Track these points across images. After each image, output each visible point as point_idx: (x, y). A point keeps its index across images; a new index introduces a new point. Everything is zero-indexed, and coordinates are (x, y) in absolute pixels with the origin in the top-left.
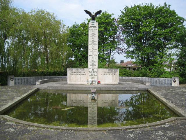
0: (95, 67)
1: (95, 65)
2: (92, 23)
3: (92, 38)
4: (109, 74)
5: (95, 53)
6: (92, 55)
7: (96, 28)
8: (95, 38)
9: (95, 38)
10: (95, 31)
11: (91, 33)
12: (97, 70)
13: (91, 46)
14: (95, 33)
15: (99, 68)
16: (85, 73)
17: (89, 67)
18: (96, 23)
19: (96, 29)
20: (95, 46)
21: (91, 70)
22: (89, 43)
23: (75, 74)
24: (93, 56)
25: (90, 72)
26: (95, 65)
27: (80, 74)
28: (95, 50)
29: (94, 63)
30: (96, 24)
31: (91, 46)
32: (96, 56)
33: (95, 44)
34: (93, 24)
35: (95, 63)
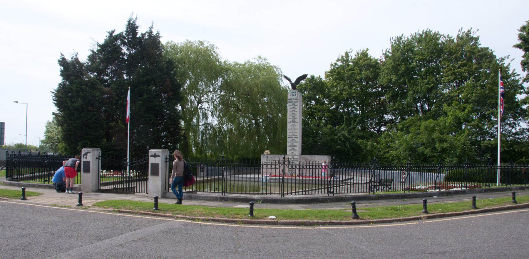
0: (295, 153)
1: (295, 150)
2: (292, 94)
3: (291, 113)
5: (295, 134)
6: (291, 137)
7: (297, 99)
8: (296, 113)
9: (296, 113)
10: (296, 104)
11: (291, 107)
12: (298, 157)
13: (291, 124)
14: (296, 107)
18: (296, 94)
19: (297, 101)
20: (296, 124)
22: (289, 120)
24: (294, 138)
26: (295, 150)
29: (294, 147)
31: (291, 124)
34: (293, 94)
35: (295, 148)
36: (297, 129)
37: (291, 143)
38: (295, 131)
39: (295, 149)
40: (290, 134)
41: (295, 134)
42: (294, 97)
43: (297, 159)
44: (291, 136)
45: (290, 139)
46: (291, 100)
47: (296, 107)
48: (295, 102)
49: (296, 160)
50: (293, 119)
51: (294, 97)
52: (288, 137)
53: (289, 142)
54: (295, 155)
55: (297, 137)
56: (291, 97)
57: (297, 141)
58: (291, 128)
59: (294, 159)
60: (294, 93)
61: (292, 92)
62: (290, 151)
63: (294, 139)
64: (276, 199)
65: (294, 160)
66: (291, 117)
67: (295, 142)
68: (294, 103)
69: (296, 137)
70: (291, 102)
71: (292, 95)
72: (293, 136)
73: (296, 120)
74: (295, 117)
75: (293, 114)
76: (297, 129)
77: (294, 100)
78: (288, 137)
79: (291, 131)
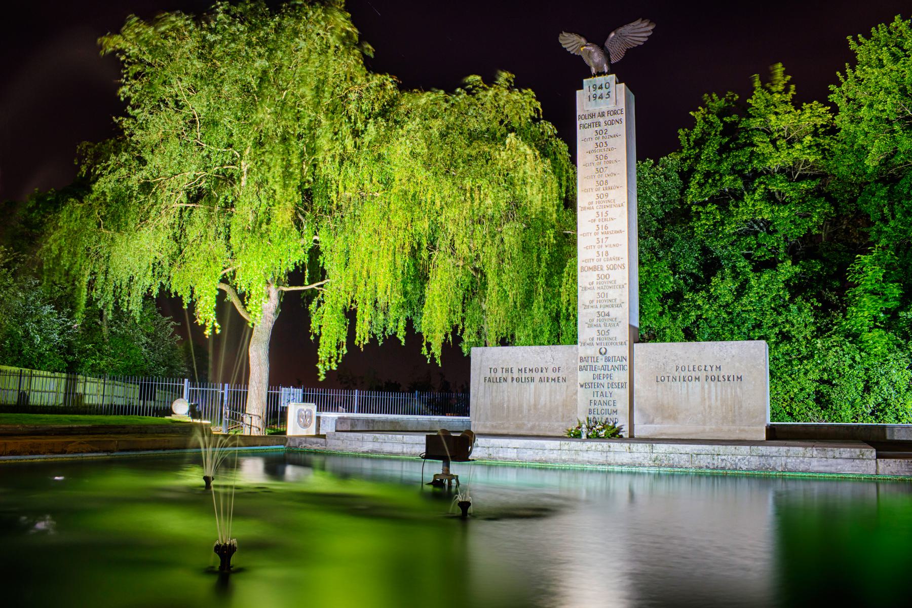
5: (613, 253)
6: (595, 268)
7: (615, 112)
9: (612, 168)
10: (612, 130)
15: (642, 340)
16: (560, 375)
17: (581, 338)
18: (612, 89)
19: (616, 117)
21: (592, 351)
24: (605, 272)
25: (586, 364)
27: (537, 380)
28: (613, 239)
29: (606, 310)
34: (599, 92)
36: (621, 231)
37: (596, 291)
38: (609, 242)
39: (612, 315)
44: (595, 263)
47: (611, 142)
52: (583, 269)
53: (585, 289)
54: (613, 342)
57: (619, 282)
58: (592, 228)
60: (601, 88)
62: (590, 326)
65: (610, 364)
69: (614, 268)
70: (590, 125)
72: (602, 263)
73: (612, 194)
74: (610, 184)
76: (621, 231)
78: (583, 269)
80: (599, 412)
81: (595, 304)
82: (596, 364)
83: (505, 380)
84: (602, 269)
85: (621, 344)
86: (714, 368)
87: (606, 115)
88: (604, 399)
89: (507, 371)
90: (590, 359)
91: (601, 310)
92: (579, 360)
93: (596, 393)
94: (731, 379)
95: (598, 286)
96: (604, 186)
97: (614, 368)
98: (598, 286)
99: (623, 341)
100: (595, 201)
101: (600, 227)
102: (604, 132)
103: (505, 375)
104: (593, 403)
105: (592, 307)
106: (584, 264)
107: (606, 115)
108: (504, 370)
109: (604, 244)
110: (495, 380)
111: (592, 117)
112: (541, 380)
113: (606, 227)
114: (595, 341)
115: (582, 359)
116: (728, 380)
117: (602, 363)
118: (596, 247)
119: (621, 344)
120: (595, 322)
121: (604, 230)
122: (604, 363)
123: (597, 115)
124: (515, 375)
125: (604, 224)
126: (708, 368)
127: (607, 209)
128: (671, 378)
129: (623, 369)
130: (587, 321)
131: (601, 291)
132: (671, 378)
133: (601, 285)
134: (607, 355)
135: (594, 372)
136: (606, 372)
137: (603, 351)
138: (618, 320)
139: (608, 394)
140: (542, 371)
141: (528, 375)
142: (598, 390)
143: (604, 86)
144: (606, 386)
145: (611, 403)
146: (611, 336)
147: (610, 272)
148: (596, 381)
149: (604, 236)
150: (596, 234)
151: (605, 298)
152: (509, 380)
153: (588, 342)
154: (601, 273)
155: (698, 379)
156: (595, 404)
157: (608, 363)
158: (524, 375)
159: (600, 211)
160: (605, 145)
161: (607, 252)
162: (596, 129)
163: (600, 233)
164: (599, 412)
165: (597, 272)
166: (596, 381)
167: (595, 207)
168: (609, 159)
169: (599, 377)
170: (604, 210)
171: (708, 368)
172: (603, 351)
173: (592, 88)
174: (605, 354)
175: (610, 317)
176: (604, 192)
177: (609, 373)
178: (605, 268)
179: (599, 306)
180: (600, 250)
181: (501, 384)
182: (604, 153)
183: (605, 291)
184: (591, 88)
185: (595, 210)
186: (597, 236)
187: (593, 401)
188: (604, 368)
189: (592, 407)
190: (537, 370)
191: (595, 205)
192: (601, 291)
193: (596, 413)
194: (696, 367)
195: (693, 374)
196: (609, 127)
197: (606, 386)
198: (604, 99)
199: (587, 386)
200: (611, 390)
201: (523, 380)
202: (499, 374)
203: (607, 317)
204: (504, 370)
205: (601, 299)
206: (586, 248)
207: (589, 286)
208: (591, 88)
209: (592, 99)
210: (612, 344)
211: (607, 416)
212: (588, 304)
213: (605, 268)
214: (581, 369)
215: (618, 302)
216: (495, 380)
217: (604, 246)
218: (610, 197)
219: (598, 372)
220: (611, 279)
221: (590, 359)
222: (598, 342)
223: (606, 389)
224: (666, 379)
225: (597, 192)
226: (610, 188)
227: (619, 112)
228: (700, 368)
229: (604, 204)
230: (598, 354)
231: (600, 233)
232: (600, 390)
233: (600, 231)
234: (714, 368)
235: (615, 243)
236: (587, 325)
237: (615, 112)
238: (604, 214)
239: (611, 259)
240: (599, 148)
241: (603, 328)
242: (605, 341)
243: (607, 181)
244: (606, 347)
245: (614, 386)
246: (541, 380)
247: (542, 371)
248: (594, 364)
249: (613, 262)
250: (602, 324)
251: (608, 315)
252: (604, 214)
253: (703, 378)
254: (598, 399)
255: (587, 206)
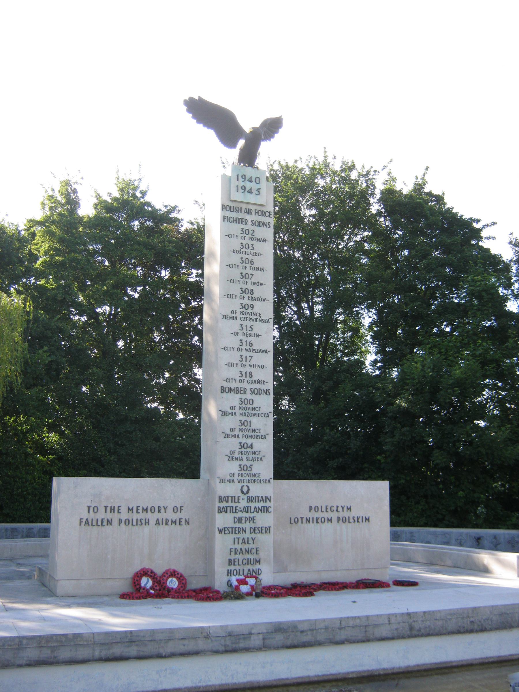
1: (258, 457)
4: (334, 516)
5: (258, 375)
6: (237, 391)
7: (263, 214)
8: (258, 276)
9: (258, 276)
13: (235, 326)
14: (259, 247)
16: (183, 515)
20: (258, 328)
23: (115, 517)
24: (248, 396)
26: (258, 457)
27: (152, 522)
28: (258, 359)
29: (249, 441)
30: (263, 191)
31: (235, 326)
32: (266, 392)
33: (257, 318)
34: (248, 185)
36: (266, 352)
38: (254, 362)
39: (255, 449)
40: (234, 373)
41: (255, 378)
42: (251, 198)
43: (267, 499)
45: (234, 399)
46: (238, 210)
47: (259, 247)
48: (253, 224)
49: (261, 505)
50: (246, 301)
51: (251, 198)
54: (256, 479)
55: (266, 392)
56: (239, 196)
57: (264, 410)
58: (234, 342)
59: (250, 500)
60: (250, 180)
61: (244, 177)
62: (231, 459)
63: (250, 402)
64: (226, 687)
65: (253, 505)
66: (238, 292)
67: (257, 413)
68: (249, 226)
69: (259, 392)
70: (235, 220)
71: (244, 188)
72: (248, 387)
73: (258, 306)
74: (256, 295)
75: (244, 276)
76: (266, 352)
77: (249, 212)
79: (237, 360)
80: (241, 563)
81: (236, 432)
82: (237, 504)
83: (110, 522)
84: (245, 393)
85: (265, 481)
86: (345, 509)
87: (253, 213)
88: (247, 546)
89: (112, 510)
90: (230, 498)
91: (244, 440)
92: (217, 500)
93: (236, 540)
94: (360, 520)
95: (241, 412)
96: (249, 295)
97: (257, 510)
98: (241, 412)
99: (268, 479)
100: (238, 310)
101: (244, 342)
102: (251, 232)
103: (109, 516)
104: (233, 553)
105: (233, 436)
106: (225, 384)
107: (253, 213)
108: (108, 509)
109: (248, 363)
110: (94, 523)
111: (238, 211)
112: (158, 523)
113: (251, 344)
114: (236, 478)
115: (221, 499)
116: (358, 522)
117: (243, 503)
118: (239, 365)
119: (265, 481)
120: (236, 455)
121: (248, 347)
122: (247, 504)
123: (243, 211)
124: (124, 515)
125: (249, 339)
126: (340, 509)
127: (252, 323)
128: (304, 520)
129: (267, 511)
130: (228, 453)
131: (243, 418)
132: (304, 520)
133: (244, 412)
134: (250, 495)
135: (235, 515)
136: (248, 515)
137: (245, 489)
138: (262, 454)
139: (251, 541)
140: (159, 511)
141: (142, 516)
142: (238, 536)
143: (253, 180)
144: (248, 531)
145: (254, 551)
146: (254, 472)
147: (253, 397)
148: (238, 525)
149: (249, 354)
150: (239, 350)
151: (248, 427)
152: (115, 522)
153: (228, 478)
154: (244, 397)
155: (330, 520)
156: (236, 553)
157: (250, 504)
158: (135, 516)
159: (244, 323)
160: (251, 248)
161: (251, 373)
162: (243, 226)
163: (244, 350)
164: (241, 563)
165: (239, 396)
166: (238, 525)
167: (238, 318)
168: (255, 265)
169: (240, 520)
170: (249, 324)
171: (340, 509)
172: (245, 489)
173: (241, 179)
174: (248, 492)
175: (253, 450)
176: (250, 302)
177: (252, 515)
178: (248, 392)
179: (241, 436)
180: (244, 370)
181: (103, 528)
182: (250, 257)
183: (249, 419)
184: (240, 177)
185: (239, 322)
186: (240, 353)
187: (233, 550)
188: (246, 510)
189: (233, 557)
190: (153, 510)
191: (238, 315)
192: (243, 418)
193: (236, 563)
194: (329, 508)
195: (326, 515)
196: (257, 229)
197: (248, 531)
198: (254, 194)
199: (227, 532)
200: (253, 535)
201: (135, 523)
202: (101, 515)
203: (249, 450)
204: (108, 509)
205: (243, 427)
206: (228, 364)
207: (230, 411)
208: (240, 177)
209: (240, 190)
210: (255, 481)
211: (249, 567)
212: (228, 432)
213: (248, 392)
214: (220, 510)
215: (262, 433)
216: (94, 523)
217: (248, 366)
218: (255, 310)
219: (240, 515)
220: (255, 405)
221: (230, 498)
222: (240, 478)
223: (247, 535)
224: (300, 520)
225: (242, 301)
226: (255, 299)
227: (268, 214)
228: (333, 508)
229: (248, 316)
230: (240, 494)
231: (244, 350)
232: (241, 536)
233: (244, 347)
234: (345, 509)
235: (261, 364)
236: (227, 458)
237: (263, 214)
238: (249, 329)
239: (255, 382)
240: (244, 249)
241: (245, 462)
242: (247, 478)
243: (252, 290)
244: (248, 484)
245: (257, 531)
246: (158, 523)
247: (159, 511)
248: (234, 505)
249: (258, 386)
250: (244, 457)
251: (251, 447)
252: (249, 329)
253: (335, 520)
254: (238, 547)
255: (230, 315)
